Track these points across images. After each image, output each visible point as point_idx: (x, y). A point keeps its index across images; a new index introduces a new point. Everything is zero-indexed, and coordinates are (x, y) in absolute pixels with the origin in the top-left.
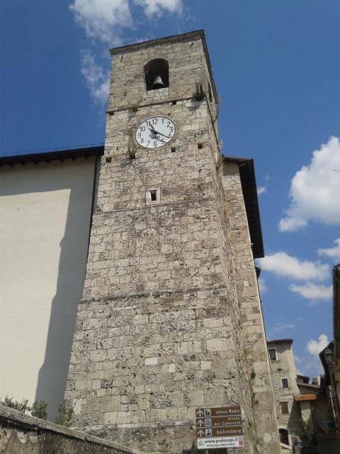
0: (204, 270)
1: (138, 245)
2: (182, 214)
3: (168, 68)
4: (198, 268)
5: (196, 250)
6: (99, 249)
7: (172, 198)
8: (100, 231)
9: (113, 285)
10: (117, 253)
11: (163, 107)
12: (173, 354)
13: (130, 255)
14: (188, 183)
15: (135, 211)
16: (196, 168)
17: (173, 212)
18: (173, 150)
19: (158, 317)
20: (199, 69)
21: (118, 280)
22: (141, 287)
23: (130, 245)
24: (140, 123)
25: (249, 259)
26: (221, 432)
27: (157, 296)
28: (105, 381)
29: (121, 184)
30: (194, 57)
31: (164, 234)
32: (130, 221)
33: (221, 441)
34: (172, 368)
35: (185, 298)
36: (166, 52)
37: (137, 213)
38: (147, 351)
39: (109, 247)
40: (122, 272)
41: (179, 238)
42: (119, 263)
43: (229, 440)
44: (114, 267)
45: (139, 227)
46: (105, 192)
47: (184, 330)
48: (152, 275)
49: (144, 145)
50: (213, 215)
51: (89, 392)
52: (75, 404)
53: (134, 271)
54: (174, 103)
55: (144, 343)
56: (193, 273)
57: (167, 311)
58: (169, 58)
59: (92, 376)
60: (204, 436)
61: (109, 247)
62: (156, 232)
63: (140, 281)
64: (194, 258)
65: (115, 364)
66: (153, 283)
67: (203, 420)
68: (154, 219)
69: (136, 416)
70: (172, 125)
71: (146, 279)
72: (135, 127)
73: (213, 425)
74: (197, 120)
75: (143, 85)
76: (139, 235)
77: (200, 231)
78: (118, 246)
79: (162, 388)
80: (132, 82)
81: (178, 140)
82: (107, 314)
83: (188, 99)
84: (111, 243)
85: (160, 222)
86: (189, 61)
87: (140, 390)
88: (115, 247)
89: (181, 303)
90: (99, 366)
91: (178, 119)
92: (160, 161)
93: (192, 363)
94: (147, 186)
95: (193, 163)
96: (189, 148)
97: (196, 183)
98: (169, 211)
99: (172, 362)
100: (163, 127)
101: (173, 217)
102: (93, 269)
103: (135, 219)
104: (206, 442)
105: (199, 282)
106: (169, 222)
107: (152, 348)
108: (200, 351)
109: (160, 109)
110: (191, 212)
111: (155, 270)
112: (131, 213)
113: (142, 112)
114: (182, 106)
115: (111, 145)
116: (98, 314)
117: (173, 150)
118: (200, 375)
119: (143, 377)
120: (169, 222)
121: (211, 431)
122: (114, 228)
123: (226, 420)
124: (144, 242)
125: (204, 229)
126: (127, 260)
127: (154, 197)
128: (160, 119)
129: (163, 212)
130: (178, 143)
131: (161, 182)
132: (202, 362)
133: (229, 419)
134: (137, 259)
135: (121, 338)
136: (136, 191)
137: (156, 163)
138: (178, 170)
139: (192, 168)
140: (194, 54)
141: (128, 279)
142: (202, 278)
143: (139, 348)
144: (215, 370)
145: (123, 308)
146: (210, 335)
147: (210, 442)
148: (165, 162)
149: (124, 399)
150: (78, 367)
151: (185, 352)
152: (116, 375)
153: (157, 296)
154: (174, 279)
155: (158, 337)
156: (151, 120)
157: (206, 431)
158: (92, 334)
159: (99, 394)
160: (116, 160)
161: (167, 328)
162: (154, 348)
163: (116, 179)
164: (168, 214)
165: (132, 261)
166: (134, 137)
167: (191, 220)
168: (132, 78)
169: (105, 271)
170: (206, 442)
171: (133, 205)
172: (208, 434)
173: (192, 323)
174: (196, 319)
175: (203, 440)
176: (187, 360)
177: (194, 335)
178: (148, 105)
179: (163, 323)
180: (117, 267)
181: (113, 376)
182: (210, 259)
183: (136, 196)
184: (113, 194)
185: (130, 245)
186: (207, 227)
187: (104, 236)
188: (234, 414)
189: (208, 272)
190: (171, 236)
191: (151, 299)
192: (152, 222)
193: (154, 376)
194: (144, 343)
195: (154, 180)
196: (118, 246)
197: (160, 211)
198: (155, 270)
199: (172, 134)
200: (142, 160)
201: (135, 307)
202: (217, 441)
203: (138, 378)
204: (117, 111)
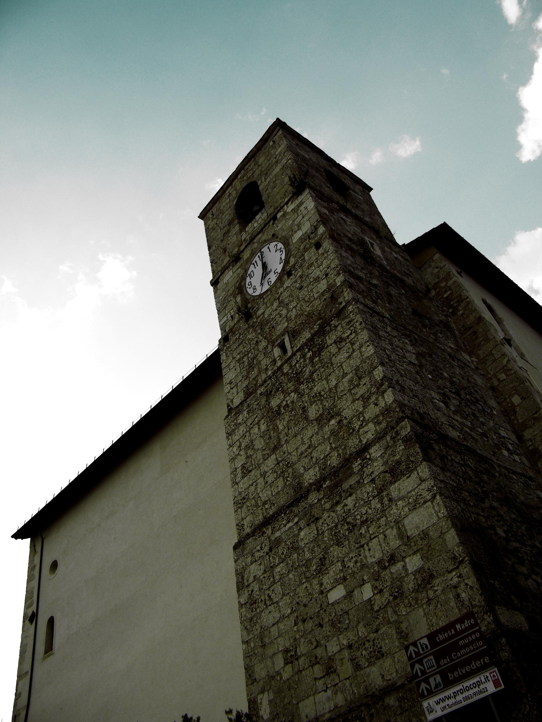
0: (372, 411)
1: (281, 427)
2: (322, 348)
4: (362, 413)
5: (354, 385)
9: (265, 503)
10: (259, 455)
12: (363, 566)
13: (275, 449)
20: (290, 161)
21: (269, 493)
25: (505, 362)
26: (456, 674)
28: (287, 651)
30: (280, 153)
33: (461, 691)
34: (367, 592)
35: (356, 470)
36: (251, 172)
38: (327, 580)
39: (250, 452)
43: (475, 685)
45: (274, 403)
47: (366, 521)
48: (307, 460)
50: (357, 324)
51: (273, 677)
52: (261, 703)
54: (275, 218)
55: (321, 569)
56: (357, 425)
57: (338, 503)
59: (270, 651)
60: (431, 693)
61: (250, 452)
64: (353, 401)
65: (292, 619)
66: (311, 472)
67: (420, 662)
68: (289, 380)
69: (339, 693)
73: (439, 666)
77: (349, 357)
79: (362, 631)
80: (228, 231)
82: (266, 549)
84: (250, 446)
85: (297, 378)
86: (277, 162)
87: (333, 647)
89: (352, 481)
90: (274, 631)
92: (279, 299)
93: (394, 569)
95: (317, 272)
97: (327, 295)
99: (364, 582)
103: (268, 395)
104: (438, 703)
106: (308, 369)
107: (331, 572)
108: (398, 543)
110: (330, 339)
111: (310, 451)
114: (284, 215)
116: (257, 554)
118: (410, 584)
119: (333, 625)
121: (438, 678)
123: (456, 647)
124: (287, 418)
125: (354, 351)
126: (273, 457)
130: (292, 261)
132: (407, 560)
133: (461, 643)
134: (285, 448)
135: (291, 576)
139: (317, 280)
140: (279, 150)
142: (371, 426)
143: (315, 582)
144: (429, 565)
146: (406, 509)
147: (443, 700)
149: (318, 670)
150: (252, 645)
151: (378, 555)
152: (297, 637)
154: (336, 448)
155: (336, 551)
157: (431, 680)
159: (285, 676)
161: (343, 530)
162: (334, 570)
164: (305, 360)
165: (278, 455)
166: (245, 292)
169: (252, 488)
170: (438, 703)
171: (264, 376)
172: (436, 686)
174: (379, 494)
175: (432, 701)
176: (385, 568)
177: (383, 521)
178: (249, 244)
179: (336, 526)
181: (295, 639)
182: (373, 390)
186: (356, 347)
188: (467, 629)
189: (377, 410)
193: (346, 617)
194: (321, 569)
198: (310, 451)
200: (260, 312)
201: (296, 520)
202: (455, 694)
203: (327, 628)
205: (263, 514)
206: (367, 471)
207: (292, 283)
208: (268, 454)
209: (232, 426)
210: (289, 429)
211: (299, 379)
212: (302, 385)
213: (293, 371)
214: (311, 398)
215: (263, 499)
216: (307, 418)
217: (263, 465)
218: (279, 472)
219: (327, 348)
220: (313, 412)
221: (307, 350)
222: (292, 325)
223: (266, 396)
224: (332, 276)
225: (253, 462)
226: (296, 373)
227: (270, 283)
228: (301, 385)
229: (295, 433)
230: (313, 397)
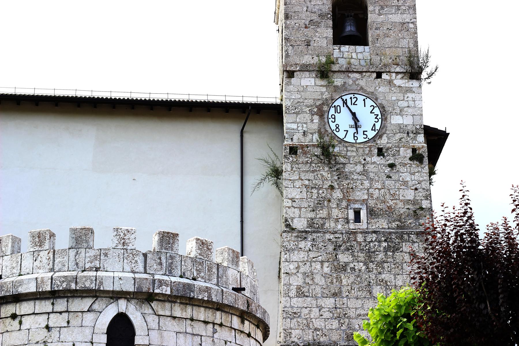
1: (344, 282)
2: (396, 249)
7: (382, 224)
9: (316, 329)
10: (318, 290)
11: (364, 80)
13: (335, 295)
14: (400, 205)
15: (337, 235)
16: (410, 183)
17: (385, 244)
23: (335, 280)
24: (333, 100)
29: (315, 191)
31: (375, 271)
32: (331, 248)
40: (327, 315)
41: (394, 281)
42: (321, 302)
44: (317, 307)
45: (344, 258)
46: (293, 200)
49: (341, 135)
54: (379, 75)
61: (308, 280)
62: (364, 268)
63: (349, 328)
70: (377, 111)
71: (357, 327)
74: (410, 110)
75: (330, 33)
76: (344, 268)
78: (319, 279)
80: (317, 24)
81: (385, 137)
83: (397, 73)
85: (370, 254)
88: (316, 281)
91: (384, 103)
94: (349, 200)
96: (401, 152)
98: (380, 242)
101: (386, 250)
102: (292, 307)
106: (381, 256)
109: (362, 83)
112: (332, 237)
115: (294, 126)
120: (381, 256)
122: (312, 255)
124: (352, 279)
126: (332, 300)
127: (357, 219)
129: (372, 241)
131: (366, 197)
136: (335, 206)
138: (388, 182)
139: (405, 183)
141: (335, 324)
148: (371, 168)
156: (348, 97)
160: (305, 153)
163: (307, 182)
166: (326, 120)
168: (315, 17)
169: (306, 311)
180: (320, 308)
183: (335, 213)
185: (335, 280)
187: (300, 264)
190: (383, 276)
192: (360, 254)
195: (358, 193)
197: (368, 239)
199: (378, 126)
204: (299, 71)
205: (313, 336)
207: (382, 164)
208: (327, 295)
209: (292, 245)
210: (351, 288)
211: (370, 257)
212: (372, 263)
213: (366, 246)
214: (378, 280)
215: (316, 326)
216: (371, 293)
217: (321, 300)
218: (335, 315)
219: (401, 252)
221: (383, 239)
222: (371, 203)
223: (334, 246)
224: (421, 194)
225: (311, 291)
226: (369, 249)
227: (356, 138)
228: (371, 262)
229: (357, 296)
230: (380, 280)
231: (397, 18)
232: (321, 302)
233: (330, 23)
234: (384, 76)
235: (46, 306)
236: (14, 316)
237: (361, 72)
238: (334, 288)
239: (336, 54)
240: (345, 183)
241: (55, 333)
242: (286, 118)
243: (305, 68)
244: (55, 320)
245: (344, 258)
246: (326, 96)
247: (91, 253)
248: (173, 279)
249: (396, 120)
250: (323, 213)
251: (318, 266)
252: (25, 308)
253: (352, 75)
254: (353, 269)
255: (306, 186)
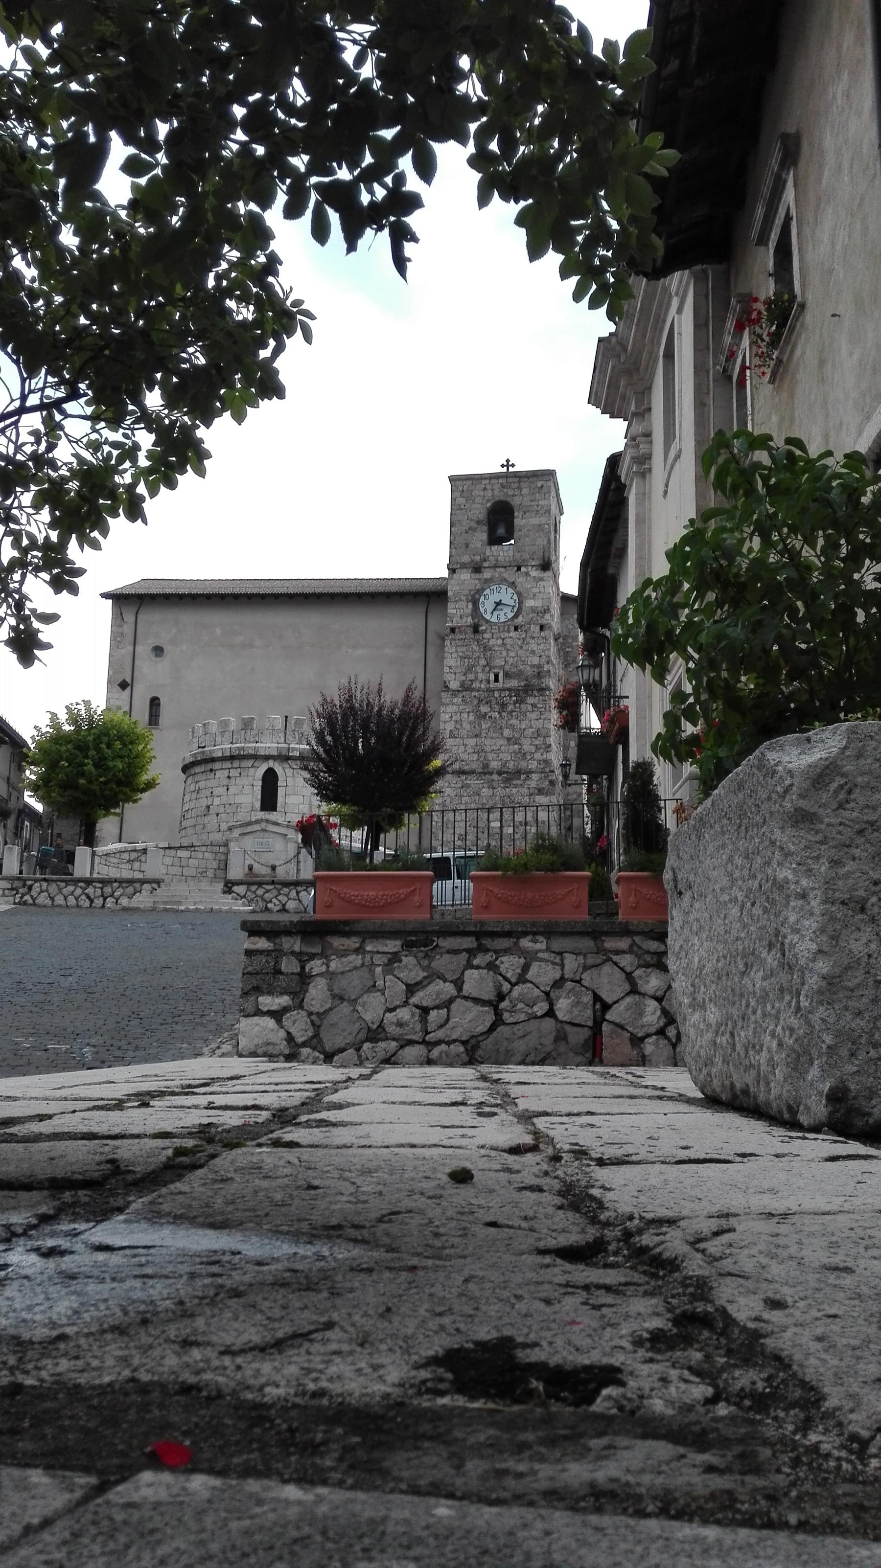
0: (538, 756)
1: (484, 727)
3: (513, 517)
6: (450, 727)
7: (513, 683)
8: (450, 709)
10: (465, 732)
13: (476, 736)
14: (528, 668)
18: (516, 629)
19: (500, 792)
22: (486, 766)
24: (483, 590)
27: (500, 773)
32: (476, 702)
37: (483, 695)
42: (466, 741)
45: (484, 709)
46: (450, 667)
49: (488, 617)
53: (479, 751)
54: (519, 569)
58: (515, 502)
68: (497, 703)
70: (515, 597)
72: (480, 592)
75: (484, 537)
78: (466, 726)
84: (459, 722)
85: (503, 706)
89: (519, 782)
91: (522, 590)
95: (534, 647)
98: (511, 697)
100: (507, 596)
101: (515, 702)
103: (480, 701)
105: (533, 765)
109: (506, 575)
110: (530, 700)
113: (487, 574)
117: (516, 629)
120: (511, 707)
127: (496, 680)
128: (504, 587)
130: (520, 620)
137: (500, 642)
139: (533, 652)
145: (473, 781)
148: (508, 641)
153: (500, 773)
158: (448, 800)
167: (530, 708)
168: (474, 524)
173: (527, 799)
180: (465, 745)
183: (481, 676)
184: (459, 670)
189: (541, 758)
191: (495, 777)
196: (466, 726)
200: (485, 636)
206: (528, 782)
220: (507, 732)
222: (507, 668)
231: (535, 521)
232: (466, 741)
233: (485, 528)
234: (523, 569)
235: (228, 764)
236: (211, 770)
237: (505, 567)
238: (477, 731)
239: (488, 553)
240: (488, 653)
241: (233, 780)
242: (450, 605)
243: (463, 566)
244: (233, 773)
245: (484, 709)
246: (478, 587)
247: (253, 732)
248: (302, 746)
249: (529, 603)
250: (471, 676)
251: (466, 715)
252: (217, 765)
253: (498, 570)
254: (490, 717)
255: (461, 657)
